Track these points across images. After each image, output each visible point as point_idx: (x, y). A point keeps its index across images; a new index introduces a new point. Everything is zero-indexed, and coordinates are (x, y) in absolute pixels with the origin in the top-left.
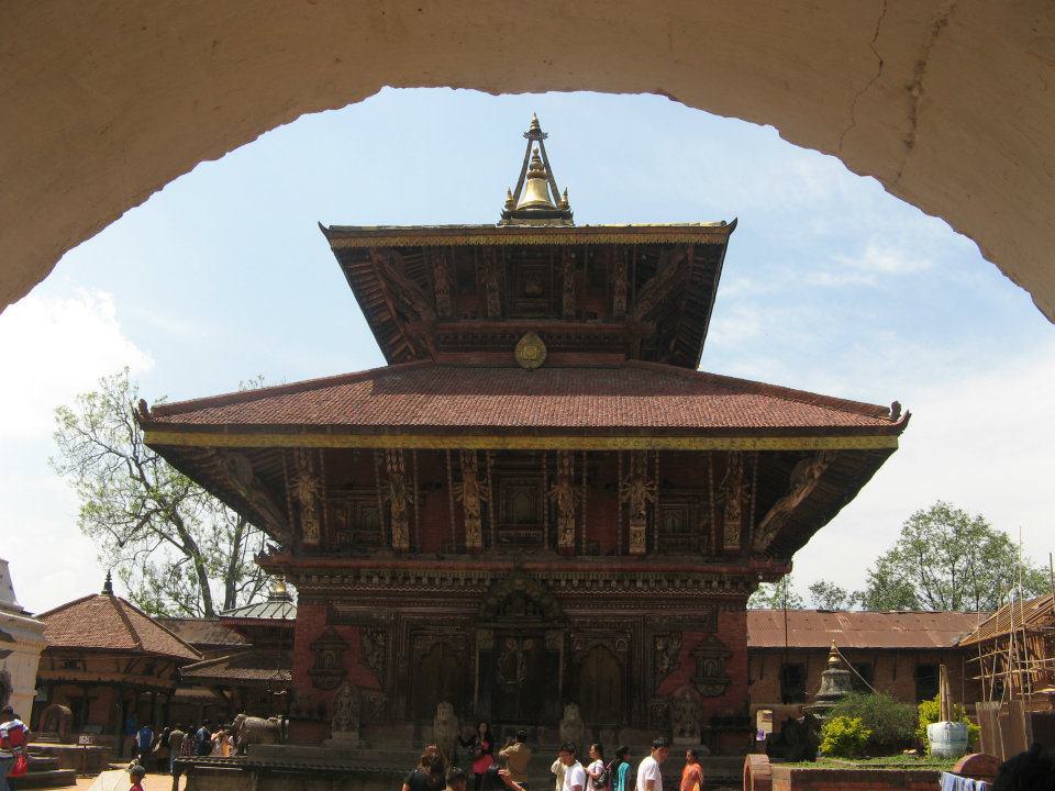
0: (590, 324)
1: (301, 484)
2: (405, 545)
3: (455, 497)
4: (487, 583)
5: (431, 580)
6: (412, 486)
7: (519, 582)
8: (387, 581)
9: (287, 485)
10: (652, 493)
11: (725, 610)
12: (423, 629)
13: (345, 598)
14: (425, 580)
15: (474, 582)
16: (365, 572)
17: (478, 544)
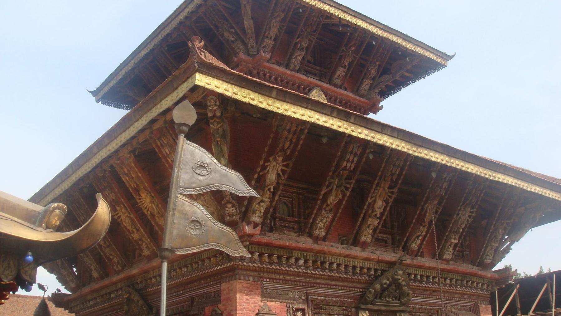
0: (345, 92)
1: (274, 163)
2: (323, 234)
3: (372, 197)
4: (372, 272)
5: (339, 265)
6: (350, 184)
7: (400, 272)
8: (310, 263)
9: (261, 163)
10: (469, 216)
11: (481, 304)
12: (321, 308)
13: (274, 277)
14: (335, 266)
15: (365, 270)
16: (296, 254)
17: (369, 240)
